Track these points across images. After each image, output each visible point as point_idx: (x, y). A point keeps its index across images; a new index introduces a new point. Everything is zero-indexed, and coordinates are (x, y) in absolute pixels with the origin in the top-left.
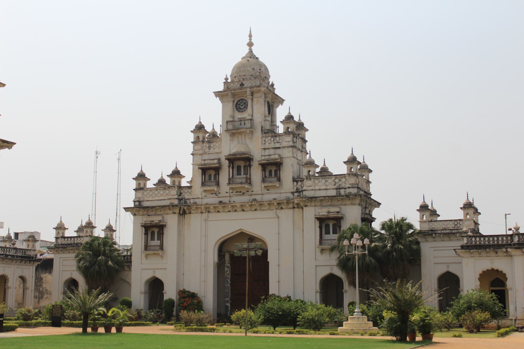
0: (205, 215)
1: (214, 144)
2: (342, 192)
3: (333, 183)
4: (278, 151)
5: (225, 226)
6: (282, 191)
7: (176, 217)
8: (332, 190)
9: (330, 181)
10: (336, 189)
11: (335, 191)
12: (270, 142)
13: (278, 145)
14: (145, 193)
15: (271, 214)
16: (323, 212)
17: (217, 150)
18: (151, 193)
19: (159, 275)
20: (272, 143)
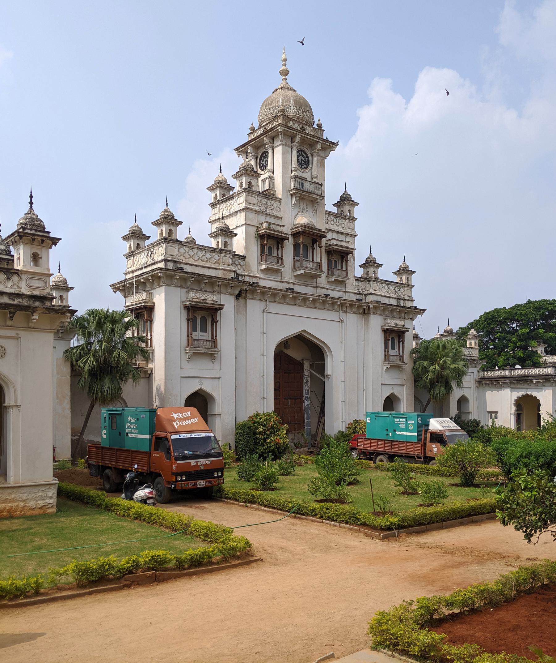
0: (263, 304)
1: (272, 202)
2: (402, 303)
3: (394, 291)
4: (342, 238)
5: (287, 322)
6: (347, 290)
7: (232, 298)
8: (394, 299)
9: (391, 288)
10: (398, 299)
11: (396, 300)
12: (332, 222)
13: (340, 229)
14: (182, 250)
15: (333, 315)
16: (392, 323)
17: (275, 213)
18: (191, 253)
19: (208, 387)
20: (335, 225)
